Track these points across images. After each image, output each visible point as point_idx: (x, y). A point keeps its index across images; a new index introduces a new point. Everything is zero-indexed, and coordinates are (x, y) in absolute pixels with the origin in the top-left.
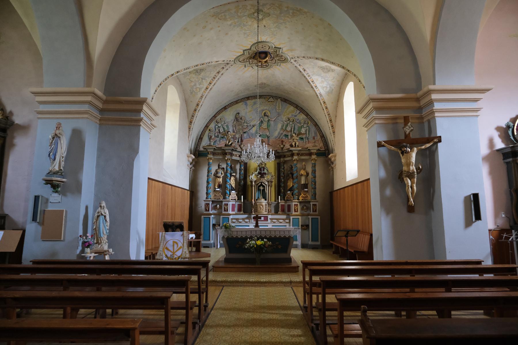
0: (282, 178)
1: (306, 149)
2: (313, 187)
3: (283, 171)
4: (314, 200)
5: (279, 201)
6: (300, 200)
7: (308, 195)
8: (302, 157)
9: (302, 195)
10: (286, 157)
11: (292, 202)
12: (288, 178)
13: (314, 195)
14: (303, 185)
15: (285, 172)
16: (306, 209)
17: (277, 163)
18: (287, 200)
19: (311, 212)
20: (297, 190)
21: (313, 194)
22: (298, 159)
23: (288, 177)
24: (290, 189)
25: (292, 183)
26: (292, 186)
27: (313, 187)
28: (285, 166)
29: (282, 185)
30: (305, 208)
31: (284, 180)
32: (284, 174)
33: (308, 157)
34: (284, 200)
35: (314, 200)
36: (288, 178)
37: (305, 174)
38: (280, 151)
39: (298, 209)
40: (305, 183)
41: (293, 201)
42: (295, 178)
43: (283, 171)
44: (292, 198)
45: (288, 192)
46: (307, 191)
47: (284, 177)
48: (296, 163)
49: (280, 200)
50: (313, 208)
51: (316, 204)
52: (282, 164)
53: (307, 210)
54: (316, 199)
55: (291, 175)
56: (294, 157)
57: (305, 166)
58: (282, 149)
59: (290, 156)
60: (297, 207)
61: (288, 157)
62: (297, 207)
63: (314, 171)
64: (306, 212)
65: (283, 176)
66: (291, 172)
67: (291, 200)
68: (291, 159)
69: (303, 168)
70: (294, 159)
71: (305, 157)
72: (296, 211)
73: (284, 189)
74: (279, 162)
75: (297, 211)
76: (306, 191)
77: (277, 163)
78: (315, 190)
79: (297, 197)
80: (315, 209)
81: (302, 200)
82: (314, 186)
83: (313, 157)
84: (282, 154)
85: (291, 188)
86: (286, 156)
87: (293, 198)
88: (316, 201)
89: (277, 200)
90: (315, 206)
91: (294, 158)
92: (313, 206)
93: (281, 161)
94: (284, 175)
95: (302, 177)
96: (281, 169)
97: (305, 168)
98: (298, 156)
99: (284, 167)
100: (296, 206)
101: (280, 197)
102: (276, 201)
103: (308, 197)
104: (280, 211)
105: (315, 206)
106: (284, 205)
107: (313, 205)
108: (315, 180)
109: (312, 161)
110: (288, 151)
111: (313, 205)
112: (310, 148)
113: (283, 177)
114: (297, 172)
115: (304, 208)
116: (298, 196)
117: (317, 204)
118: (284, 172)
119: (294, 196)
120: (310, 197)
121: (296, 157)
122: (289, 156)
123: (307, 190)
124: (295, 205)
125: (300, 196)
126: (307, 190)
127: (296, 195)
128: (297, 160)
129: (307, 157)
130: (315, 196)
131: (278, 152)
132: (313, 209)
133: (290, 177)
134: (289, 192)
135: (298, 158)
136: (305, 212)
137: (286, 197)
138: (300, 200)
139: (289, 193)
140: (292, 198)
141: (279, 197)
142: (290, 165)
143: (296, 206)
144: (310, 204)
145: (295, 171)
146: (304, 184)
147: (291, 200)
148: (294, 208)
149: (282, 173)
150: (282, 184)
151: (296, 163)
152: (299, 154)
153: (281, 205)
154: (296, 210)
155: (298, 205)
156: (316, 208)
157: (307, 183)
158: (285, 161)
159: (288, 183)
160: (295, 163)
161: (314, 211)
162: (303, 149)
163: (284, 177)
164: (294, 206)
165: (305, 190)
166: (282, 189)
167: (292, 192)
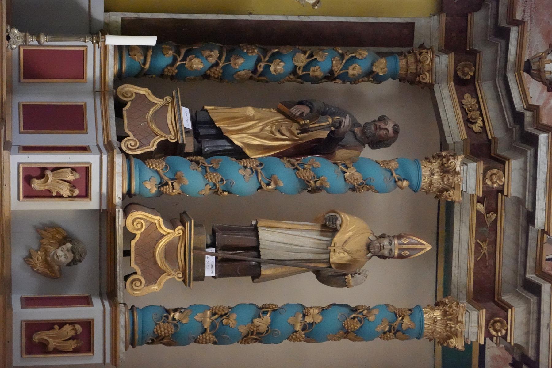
0: (301, 60)
1: (530, 262)
2: (232, 321)
3: (355, 70)
4: (122, 333)
5: (112, 41)
6: (126, 214)
7: (164, 279)
8: (465, 232)
9: (164, 229)
10: (461, 98)
11: (109, 148)
12: (296, 110)
13: (166, 329)
14: (248, 240)
15: (337, 86)
16: (47, 263)
17: (411, 26)
18: (119, 105)
19: (28, 302)
20: (206, 190)
21: (176, 324)
22: (454, 195)
23: (306, 110)
24: (211, 123)
25: (256, 142)
26: (237, 139)
27: (232, 321)
28: (389, 86)
29: (240, 61)
30: (60, 252)
31: (278, 79)
32: (331, 76)
33: (463, 279)
34: (120, 78)
35: (122, 333)
36: (296, 110)
37: (338, 257)
38: (512, 50)
39: (47, 195)
40: (265, 254)
41: (119, 160)
42: (307, 174)
43: (355, 70)
44: (143, 143)
45: (185, 112)
46: (200, 277)
47: (305, 78)
48: (425, 182)
49: (119, 49)
50: (62, 324)
51: (88, 348)
52: (402, 63)
53: (40, 267)
54: (132, 342)
55: (324, 135)
56: (473, 166)
57: (400, 257)
58: (528, 70)
59: (469, 130)
60: (65, 191)
61: (465, 113)
62: (65, 191)
63: (356, 332)
64: (28, 259)
65: (317, 71)
66: (349, 139)
67: (120, 138)
68: (449, 140)
69: (386, 242)
70: (457, 163)
71: (464, 245)
72: (28, 179)
73: (206, 76)
74: (417, 41)
75: (30, 194)
76: (200, 263)
77: (411, 26)
78: (209, 336)
79: (151, 188)
80: (52, 344)
81: (129, 236)
82: (243, 329)
83: (474, 315)
84: (485, 69)
85: (220, 135)
86: (468, 99)
87: (145, 157)
88: (121, 346)
89: (116, 17)
90: (73, 345)
91: (463, 164)
92: (72, 323)
93: (429, 56)
94: (316, 80)
95: (316, 235)
96: (364, 53)
97: (383, 257)
98: (480, 200)
99: (378, 79)
100: (73, 185)
101: (146, 48)
102: (106, 10)
103: (151, 280)
104: (33, 42)
105: (73, 345)
106: (81, 75)
107: (88, 325)
108: (292, 336)
109: (437, 313)
110: (518, 117)
111: (88, 325)
112: (545, 296)
113: (306, 67)
114: (354, 189)
115: (61, 243)
116: (160, 193)
117: (97, 358)
118: (344, 77)
119: (159, 165)
120: (154, 293)
121: (472, 182)
122: (468, 122)
123: (210, 271)
124: (86, 171)
125: (157, 219)
126: (210, 271)
127: (162, 184)
128: (452, 187)
129: (464, 265)
130: (157, 339)
131: (504, 34)
132: (49, 325)
133: (304, 130)
134: (187, 123)
135: (463, 193)
136: (25, 253)
137: (144, 91)
138: (126, 214)
139: (178, 118)
140: (143, 143)
141: (151, 41)
142: (396, 131)
143: (73, 185)
144: (86, 301)
145: (357, 175)
146: (256, 248)
147: (120, 138)
148: (54, 170)
149: (338, 67)
150: (251, 64)
151: (425, 182)
152: (493, 209)
153: (81, 55)
154: (37, 185)
155: (86, 195)
156: (56, 351)
157: (266, 271)
158: (430, 87)
159: (256, 106)
160: (426, 172)
161: (36, 338)
162: (532, 243)
163: (305, 78)
164: (73, 169)
165: (210, 261)
166: (212, 60)
167: (189, 148)
